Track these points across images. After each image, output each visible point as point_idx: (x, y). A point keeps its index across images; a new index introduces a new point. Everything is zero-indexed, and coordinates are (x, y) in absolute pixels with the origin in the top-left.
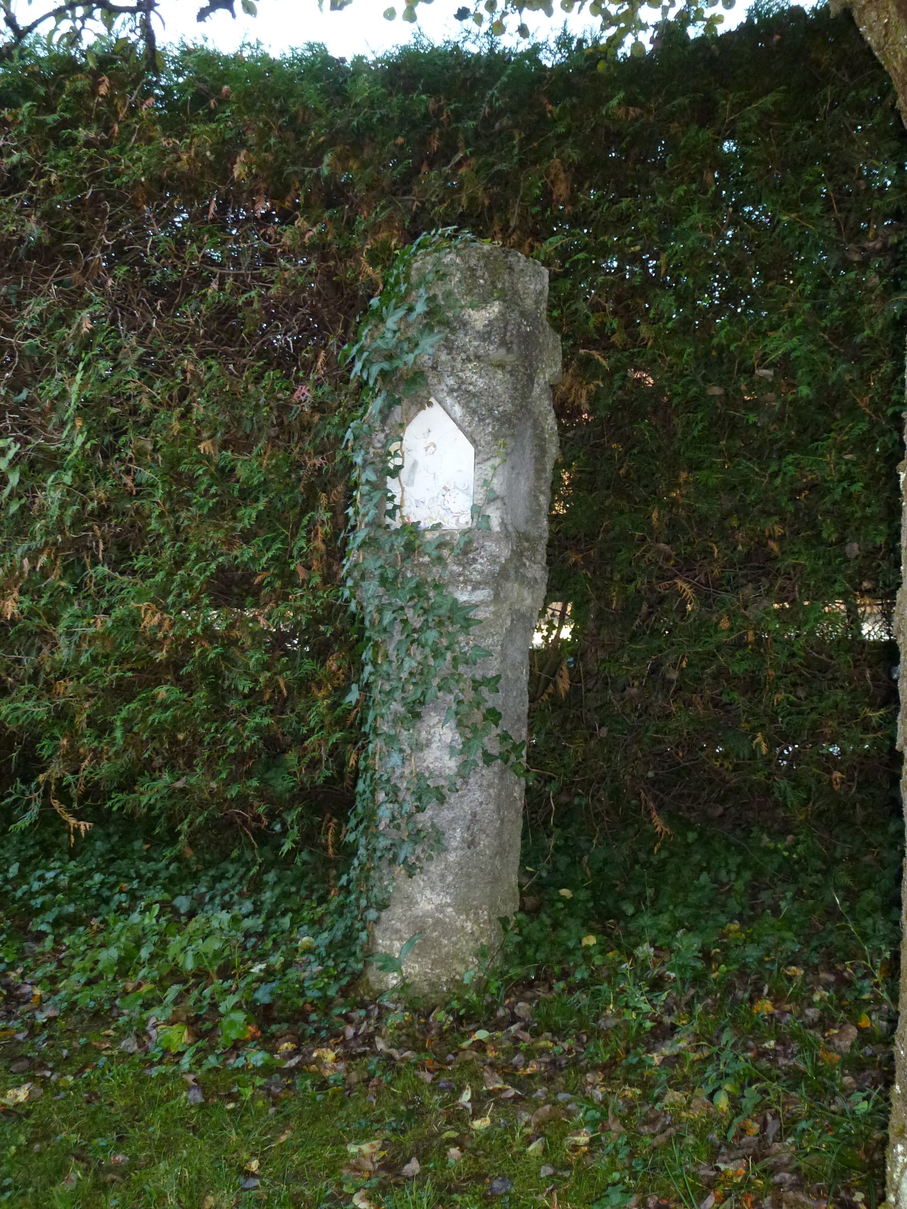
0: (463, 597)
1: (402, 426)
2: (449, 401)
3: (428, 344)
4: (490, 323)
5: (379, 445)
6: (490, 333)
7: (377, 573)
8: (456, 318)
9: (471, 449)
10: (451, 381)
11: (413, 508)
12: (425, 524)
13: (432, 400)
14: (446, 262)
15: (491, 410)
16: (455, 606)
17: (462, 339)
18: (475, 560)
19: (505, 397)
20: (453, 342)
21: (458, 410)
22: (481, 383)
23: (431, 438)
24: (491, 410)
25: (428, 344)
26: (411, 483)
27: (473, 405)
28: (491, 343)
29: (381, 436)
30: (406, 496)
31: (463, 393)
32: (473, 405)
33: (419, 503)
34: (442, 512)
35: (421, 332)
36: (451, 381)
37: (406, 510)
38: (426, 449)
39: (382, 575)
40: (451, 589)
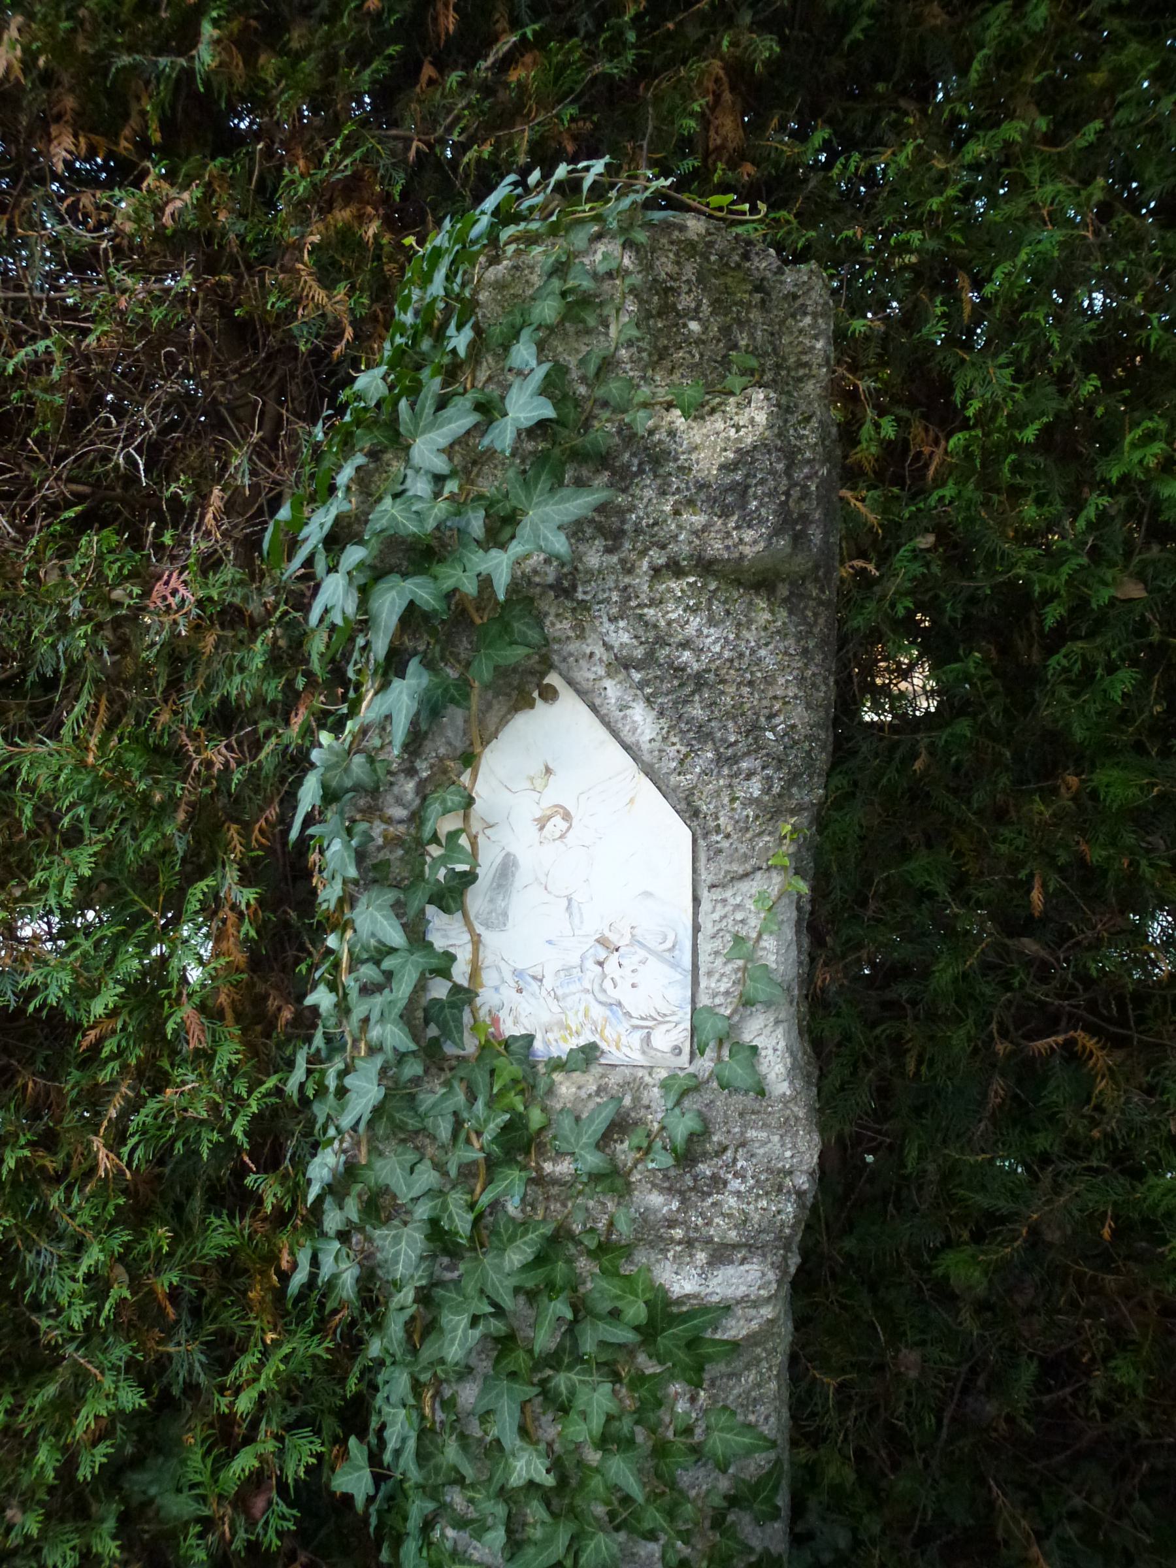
0: (682, 1281)
1: (469, 759)
2: (612, 690)
3: (548, 525)
4: (744, 458)
5: (399, 813)
6: (741, 490)
7: (422, 1211)
8: (628, 436)
9: (682, 834)
10: (622, 636)
11: (508, 994)
12: (553, 1045)
13: (553, 679)
14: (559, 259)
15: (754, 729)
16: (663, 1314)
17: (648, 502)
18: (718, 1184)
19: (785, 685)
20: (622, 512)
21: (643, 723)
22: (713, 640)
23: (557, 792)
24: (754, 729)
25: (548, 525)
26: (500, 920)
27: (697, 711)
28: (747, 522)
29: (409, 787)
30: (488, 957)
31: (658, 670)
32: (697, 711)
33: (523, 980)
34: (598, 1012)
35: (527, 483)
36: (622, 636)
37: (487, 998)
38: (542, 823)
39: (434, 1222)
40: (642, 1256)
